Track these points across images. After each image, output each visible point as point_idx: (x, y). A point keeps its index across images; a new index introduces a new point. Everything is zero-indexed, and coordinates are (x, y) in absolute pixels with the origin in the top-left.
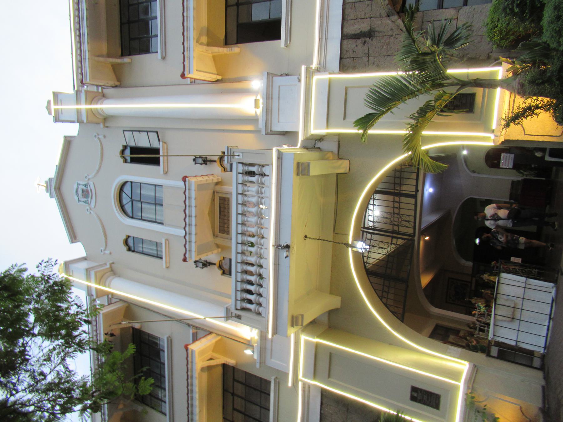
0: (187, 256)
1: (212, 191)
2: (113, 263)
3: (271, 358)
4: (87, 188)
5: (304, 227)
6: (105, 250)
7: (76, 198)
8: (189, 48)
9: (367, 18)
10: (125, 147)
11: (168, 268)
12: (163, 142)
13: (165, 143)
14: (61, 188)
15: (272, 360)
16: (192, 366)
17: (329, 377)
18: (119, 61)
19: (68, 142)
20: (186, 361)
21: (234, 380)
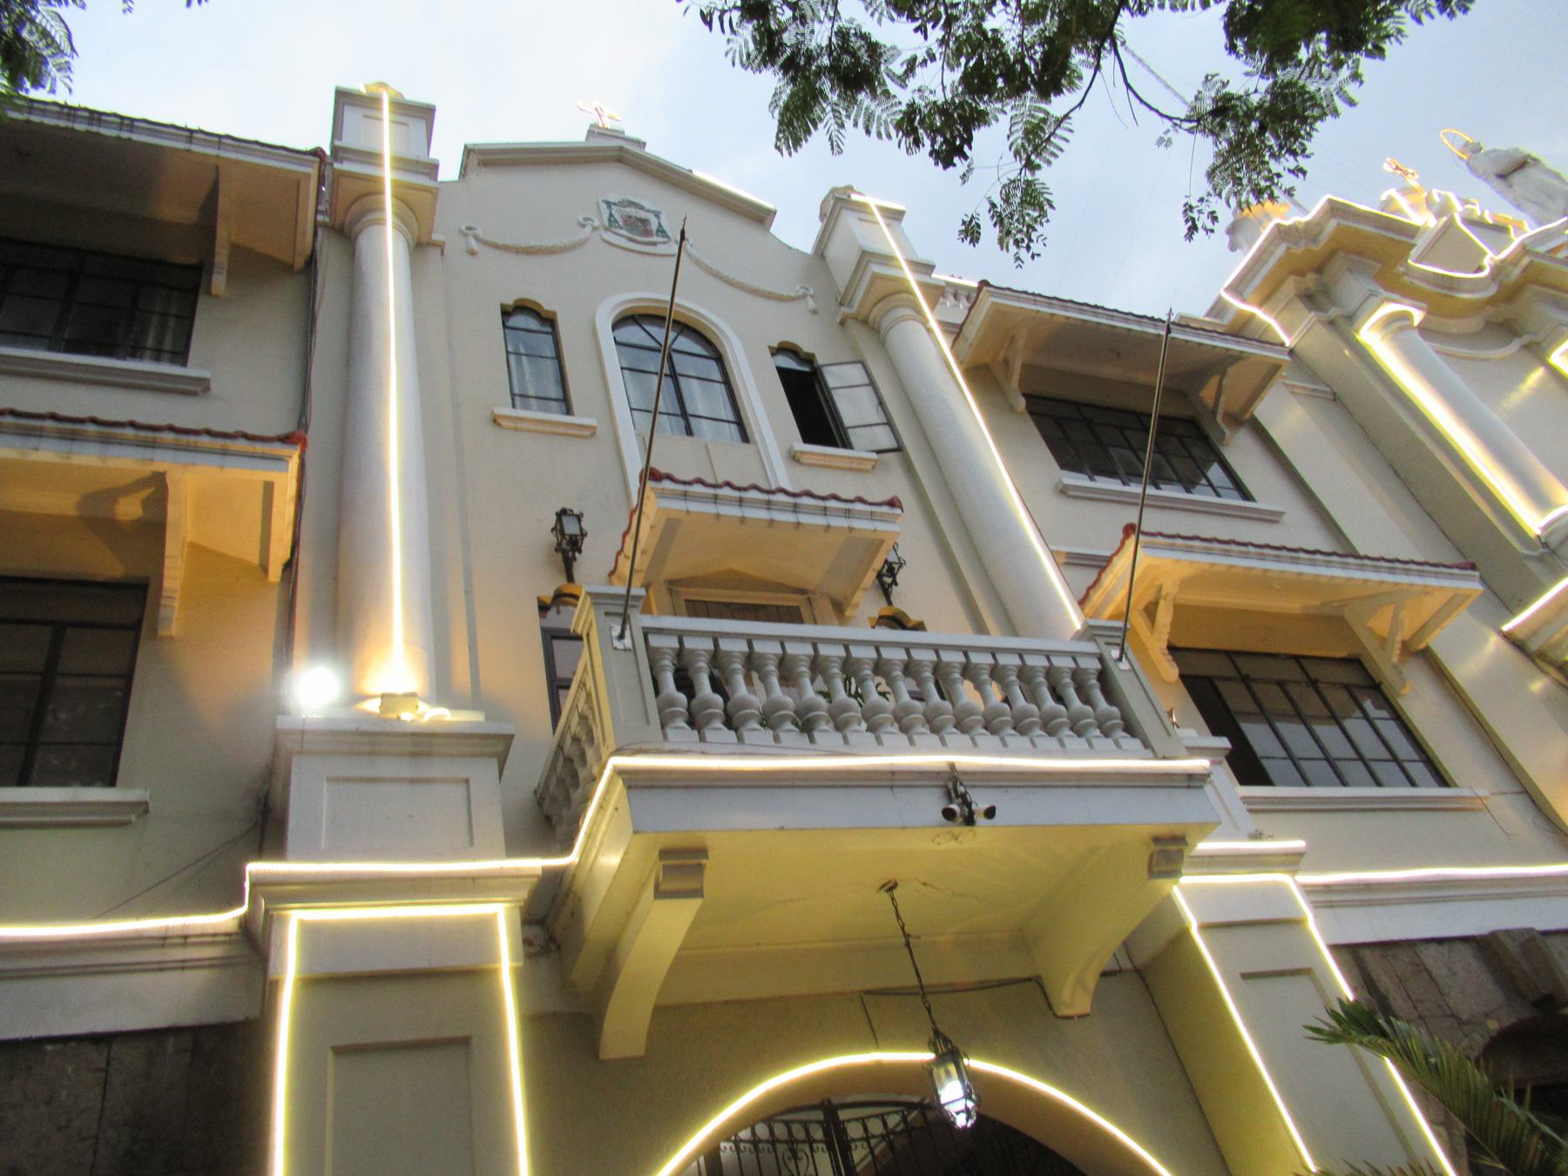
0: (667, 484)
1: (810, 588)
2: (442, 253)
3: (331, 780)
4: (658, 235)
5: (923, 880)
6: (476, 238)
7: (613, 198)
8: (1190, 550)
9: (1415, 1008)
10: (808, 359)
11: (495, 421)
12: (876, 461)
13: (874, 467)
14: (619, 164)
15: (325, 786)
16: (211, 452)
17: (339, 1051)
18: (1015, 384)
19: (760, 217)
20: (231, 430)
21: (59, 629)
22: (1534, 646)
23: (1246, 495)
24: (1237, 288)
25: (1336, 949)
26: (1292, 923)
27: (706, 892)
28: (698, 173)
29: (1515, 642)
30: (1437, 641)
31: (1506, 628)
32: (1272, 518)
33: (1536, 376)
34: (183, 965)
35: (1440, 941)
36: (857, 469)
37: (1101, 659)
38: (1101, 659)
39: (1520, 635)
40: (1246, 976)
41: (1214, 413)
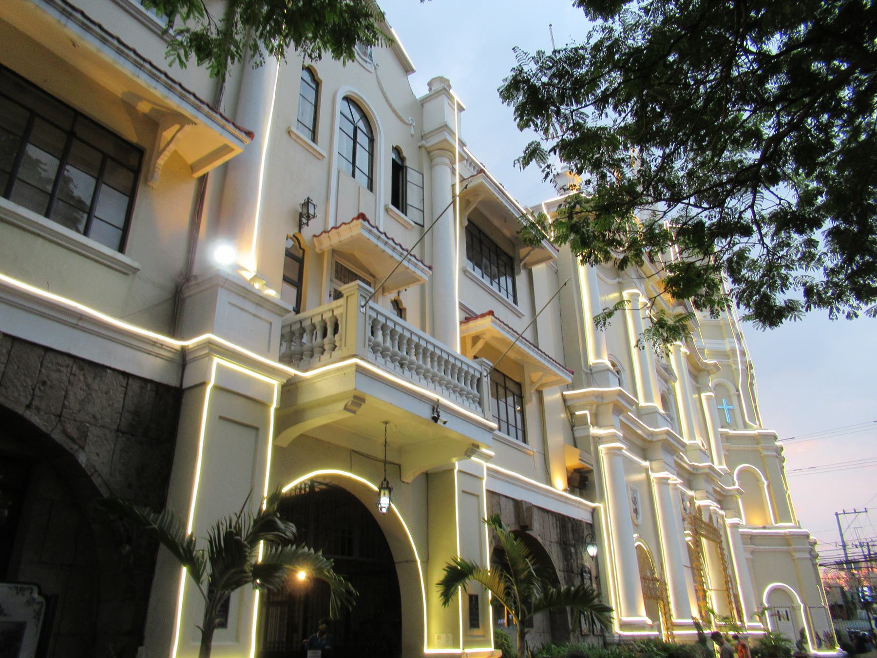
0: (366, 224)
1: (377, 276)
11: (289, 132)
17: (221, 418)
19: (407, 69)
22: (569, 403)
23: (515, 302)
24: (549, 205)
25: (488, 491)
26: (479, 478)
27: (357, 413)
28: (393, 30)
29: (564, 399)
30: (545, 391)
31: (565, 393)
32: (519, 315)
33: (616, 295)
34: (157, 356)
35: (506, 497)
36: (405, 226)
37: (481, 374)
38: (481, 374)
39: (567, 398)
40: (463, 492)
41: (521, 261)
